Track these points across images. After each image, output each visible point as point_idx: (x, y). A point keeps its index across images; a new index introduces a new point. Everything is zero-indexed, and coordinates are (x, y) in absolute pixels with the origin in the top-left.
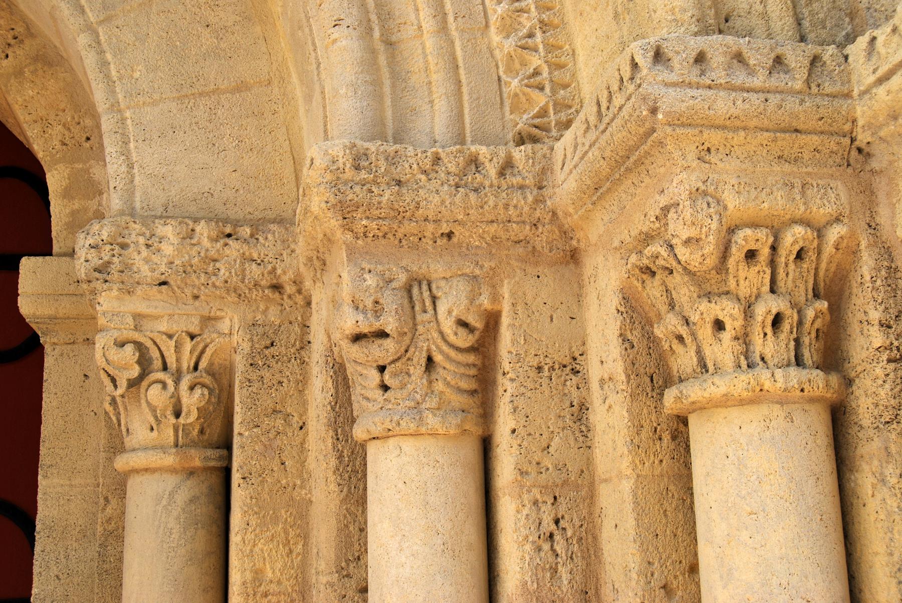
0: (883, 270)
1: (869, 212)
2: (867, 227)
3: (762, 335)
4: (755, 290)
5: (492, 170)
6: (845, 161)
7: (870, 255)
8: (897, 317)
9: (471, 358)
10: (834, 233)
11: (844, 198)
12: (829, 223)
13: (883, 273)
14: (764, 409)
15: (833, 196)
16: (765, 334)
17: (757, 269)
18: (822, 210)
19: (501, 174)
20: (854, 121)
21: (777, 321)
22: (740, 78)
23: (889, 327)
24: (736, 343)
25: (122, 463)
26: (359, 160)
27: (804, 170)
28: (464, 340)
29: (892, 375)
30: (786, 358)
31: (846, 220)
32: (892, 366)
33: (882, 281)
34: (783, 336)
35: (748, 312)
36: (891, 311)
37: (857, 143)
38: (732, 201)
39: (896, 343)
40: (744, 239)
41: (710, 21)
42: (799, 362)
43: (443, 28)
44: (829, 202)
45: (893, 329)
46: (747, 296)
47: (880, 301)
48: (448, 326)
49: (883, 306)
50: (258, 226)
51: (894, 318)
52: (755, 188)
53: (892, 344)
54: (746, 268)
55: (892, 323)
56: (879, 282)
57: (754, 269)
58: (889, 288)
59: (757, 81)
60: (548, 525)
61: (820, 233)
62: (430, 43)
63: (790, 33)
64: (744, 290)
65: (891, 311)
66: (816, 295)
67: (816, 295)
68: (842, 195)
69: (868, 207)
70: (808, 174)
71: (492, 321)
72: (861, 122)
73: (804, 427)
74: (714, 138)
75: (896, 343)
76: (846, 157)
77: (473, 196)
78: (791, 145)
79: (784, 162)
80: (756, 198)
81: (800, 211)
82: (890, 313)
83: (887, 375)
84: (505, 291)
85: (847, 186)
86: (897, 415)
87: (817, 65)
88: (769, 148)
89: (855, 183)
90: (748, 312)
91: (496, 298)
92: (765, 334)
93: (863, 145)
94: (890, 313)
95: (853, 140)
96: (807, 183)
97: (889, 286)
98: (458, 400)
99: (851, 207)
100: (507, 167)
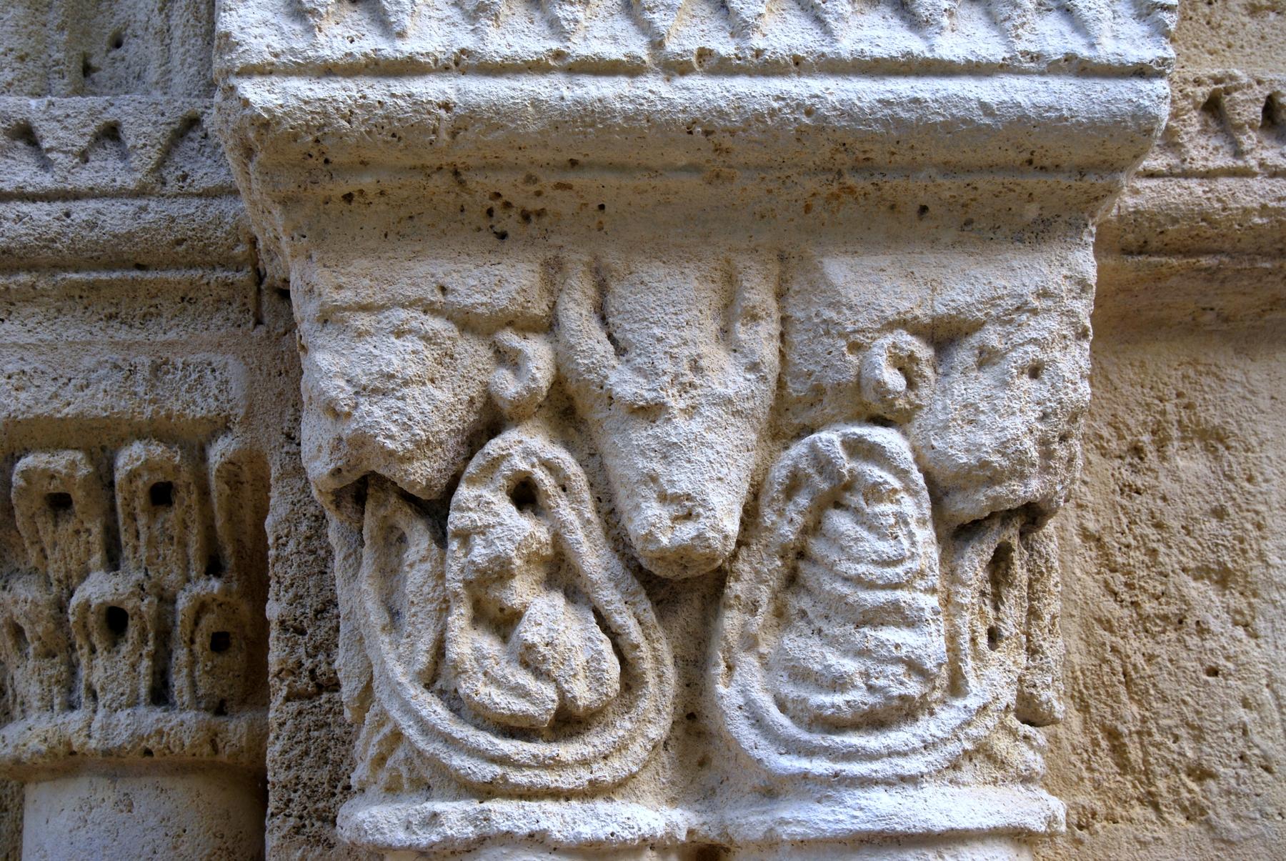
0: (305, 523)
1: (291, 411)
2: (282, 439)
3: (86, 650)
4: (74, 566)
6: (250, 316)
7: (282, 494)
8: (317, 612)
10: (219, 452)
11: (237, 390)
12: (213, 437)
13: (303, 528)
15: (214, 384)
16: (93, 650)
17: (71, 527)
20: (253, 242)
23: (302, 632)
24: (46, 663)
27: (161, 338)
29: (289, 723)
30: (128, 691)
31: (236, 429)
32: (294, 706)
33: (299, 544)
34: (125, 648)
36: (308, 601)
37: (267, 280)
39: (308, 664)
41: (57, 56)
42: (160, 695)
44: (205, 397)
45: (307, 637)
46: (61, 575)
47: (288, 582)
49: (291, 594)
51: (311, 615)
52: (55, 379)
53: (300, 664)
54: (50, 527)
55: (305, 625)
56: (291, 546)
57: (67, 528)
58: (312, 558)
63: (193, 70)
65: (308, 601)
68: (233, 384)
69: (291, 402)
70: (170, 344)
72: (261, 245)
73: (152, 821)
75: (308, 664)
76: (252, 310)
78: (132, 295)
79: (118, 326)
80: (55, 396)
82: (303, 606)
83: (281, 725)
85: (246, 364)
86: (290, 800)
87: (191, 135)
88: (85, 301)
89: (267, 358)
92: (93, 650)
93: (279, 284)
94: (303, 606)
95: (259, 277)
96: (165, 363)
97: (313, 552)
99: (251, 406)
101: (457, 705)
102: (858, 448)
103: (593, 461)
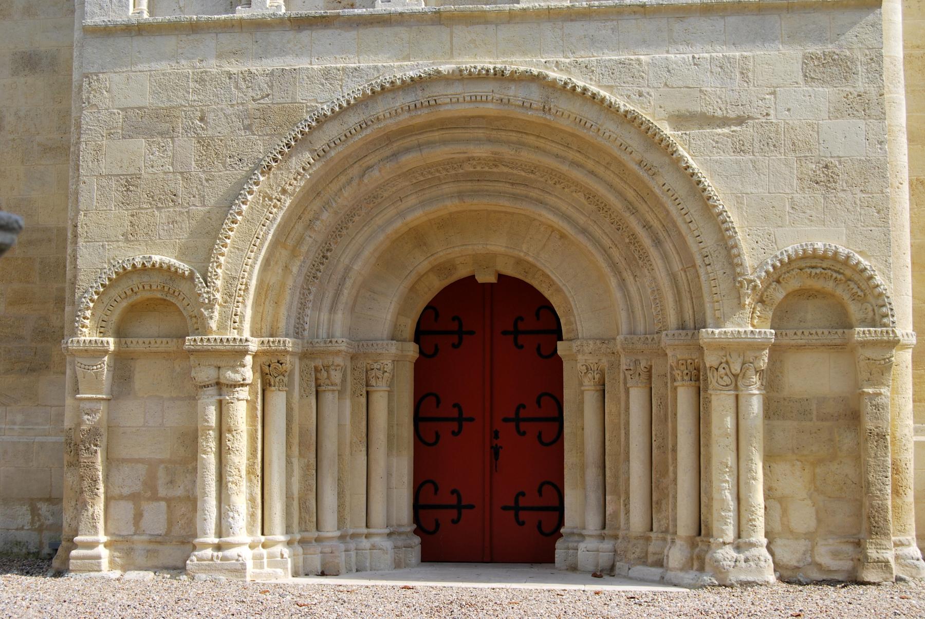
5: (650, 340)
9: (647, 373)
10: (696, 361)
14: (684, 387)
18: (694, 357)
19: (652, 341)
21: (687, 374)
22: (680, 338)
25: (583, 388)
26: (626, 339)
28: (646, 370)
35: (682, 373)
38: (678, 356)
40: (681, 362)
42: (691, 380)
43: (643, 309)
48: (642, 368)
50: (609, 340)
59: (683, 338)
60: (659, 403)
61: (694, 360)
62: (640, 312)
64: (682, 369)
66: (695, 369)
67: (695, 369)
71: (651, 367)
74: (676, 347)
77: (646, 346)
81: (690, 357)
84: (653, 362)
90: (682, 373)
91: (651, 363)
98: (645, 381)
100: (653, 338)
101: (718, 383)
102: (749, 366)
103: (729, 366)
